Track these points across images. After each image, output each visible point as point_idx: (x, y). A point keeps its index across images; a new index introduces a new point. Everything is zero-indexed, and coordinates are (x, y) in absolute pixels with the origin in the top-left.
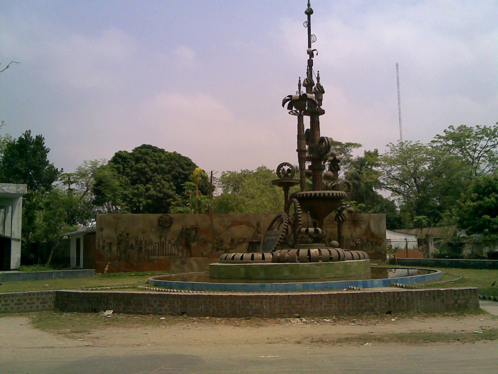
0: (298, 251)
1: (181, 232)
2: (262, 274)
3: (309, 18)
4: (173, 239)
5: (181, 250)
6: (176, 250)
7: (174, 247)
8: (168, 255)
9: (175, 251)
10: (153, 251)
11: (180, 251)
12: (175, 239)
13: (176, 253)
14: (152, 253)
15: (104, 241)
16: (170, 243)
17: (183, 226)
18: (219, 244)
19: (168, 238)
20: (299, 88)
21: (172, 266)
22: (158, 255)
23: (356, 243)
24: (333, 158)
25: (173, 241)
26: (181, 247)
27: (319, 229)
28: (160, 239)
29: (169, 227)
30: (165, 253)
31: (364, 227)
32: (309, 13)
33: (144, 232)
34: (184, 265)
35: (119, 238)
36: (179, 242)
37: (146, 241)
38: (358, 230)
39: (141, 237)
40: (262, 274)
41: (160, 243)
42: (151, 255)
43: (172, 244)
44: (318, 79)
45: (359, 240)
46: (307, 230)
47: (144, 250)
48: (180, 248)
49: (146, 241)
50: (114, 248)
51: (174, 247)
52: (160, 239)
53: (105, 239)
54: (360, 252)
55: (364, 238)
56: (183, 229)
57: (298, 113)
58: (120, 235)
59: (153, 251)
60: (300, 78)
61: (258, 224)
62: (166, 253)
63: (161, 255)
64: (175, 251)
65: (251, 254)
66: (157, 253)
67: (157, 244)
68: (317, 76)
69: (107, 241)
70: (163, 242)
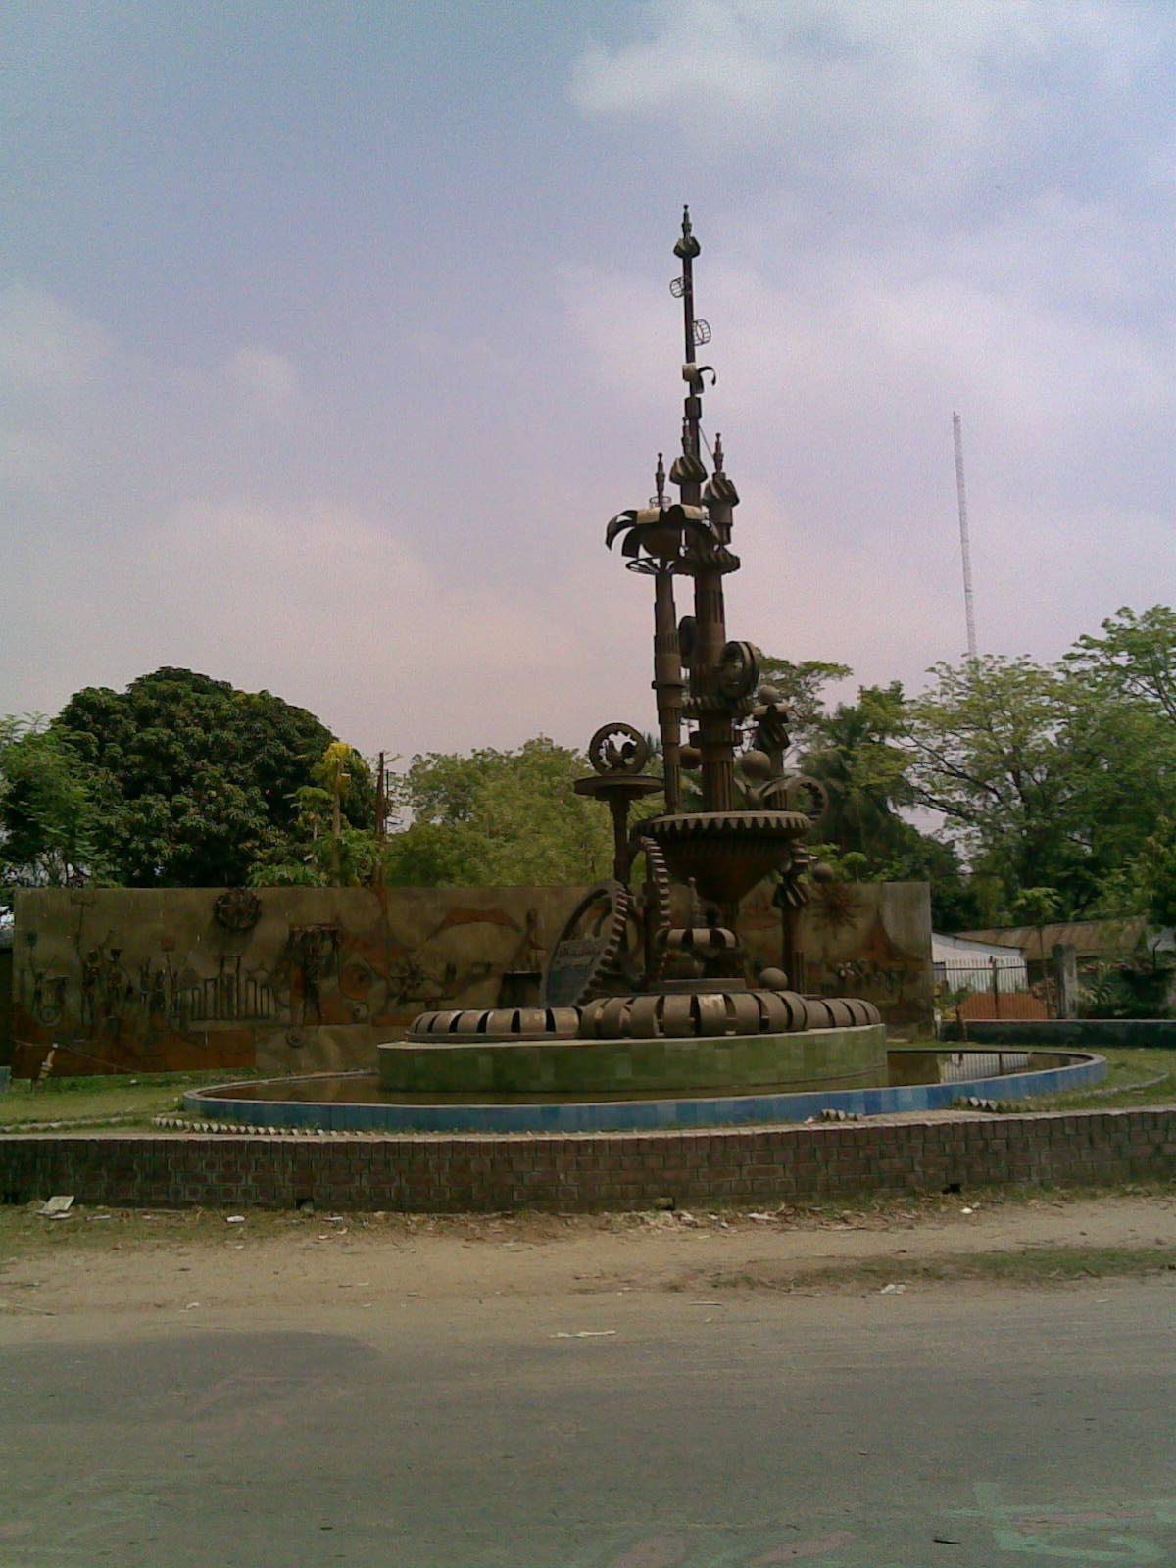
0: (661, 1001)
1: (289, 945)
2: (547, 1078)
3: (687, 269)
4: (261, 967)
6: (272, 1003)
9: (266, 1004)
10: (196, 1010)
11: (285, 1006)
12: (269, 969)
13: (272, 1011)
14: (196, 1015)
15: (39, 977)
17: (292, 926)
18: (409, 981)
19: (247, 963)
20: (658, 490)
22: (215, 1019)
23: (839, 974)
24: (769, 708)
25: (261, 975)
26: (289, 992)
27: (726, 933)
29: (249, 930)
31: (862, 923)
32: (688, 251)
33: (168, 946)
35: (89, 965)
38: (845, 935)
39: (160, 962)
40: (547, 1078)
41: (219, 981)
42: (193, 1020)
44: (718, 458)
45: (849, 965)
46: (688, 937)
47: (168, 1001)
48: (285, 996)
49: (176, 974)
50: (73, 999)
51: (264, 992)
52: (222, 967)
53: (42, 970)
54: (855, 1004)
55: (863, 959)
56: (292, 934)
57: (654, 565)
58: (93, 957)
60: (660, 455)
61: (531, 919)
63: (223, 1018)
64: (266, 1004)
65: (512, 1012)
67: (209, 985)
68: (714, 450)
69: (51, 976)
70: (230, 978)
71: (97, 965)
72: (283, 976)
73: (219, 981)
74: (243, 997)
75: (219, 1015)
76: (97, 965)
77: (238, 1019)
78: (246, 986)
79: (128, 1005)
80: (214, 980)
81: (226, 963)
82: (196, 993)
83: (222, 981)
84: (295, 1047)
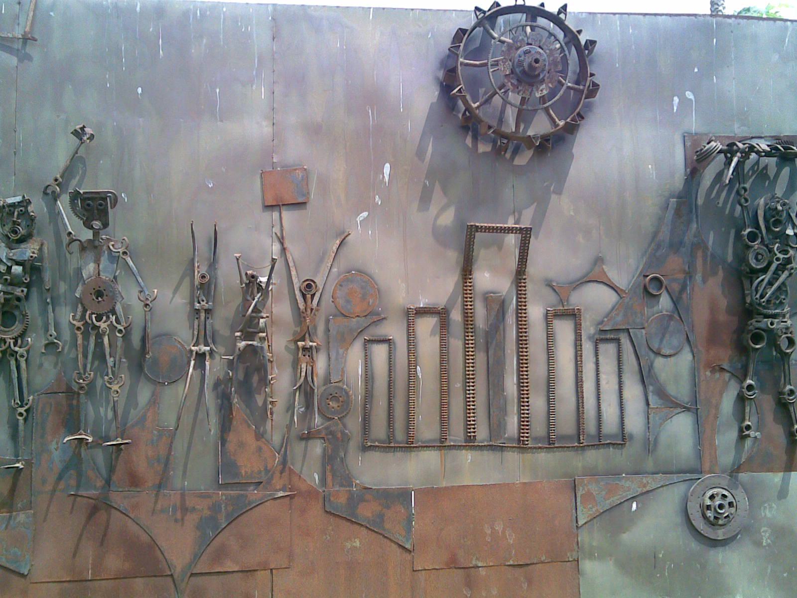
5: (681, 390)
6: (633, 392)
7: (608, 351)
8: (550, 442)
10: (380, 403)
11: (673, 404)
12: (622, 277)
13: (635, 423)
14: (379, 430)
16: (574, 315)
17: (691, 141)
21: (588, 566)
22: (442, 444)
26: (686, 357)
28: (467, 271)
30: (512, 423)
34: (719, 555)
36: (665, 302)
37: (309, 285)
41: (456, 316)
42: (365, 449)
43: (588, 328)
49: (309, 285)
52: (467, 271)
59: (380, 403)
62: (524, 422)
63: (470, 442)
66: (427, 430)
67: (426, 326)
71: (28, 251)
72: (665, 302)
73: (456, 316)
74: (537, 370)
75: (457, 434)
76: (28, 251)
77: (521, 445)
78: (550, 337)
79: (144, 394)
80: (442, 314)
81: (482, 255)
82: (380, 352)
83: (468, 317)
84: (715, 543)
